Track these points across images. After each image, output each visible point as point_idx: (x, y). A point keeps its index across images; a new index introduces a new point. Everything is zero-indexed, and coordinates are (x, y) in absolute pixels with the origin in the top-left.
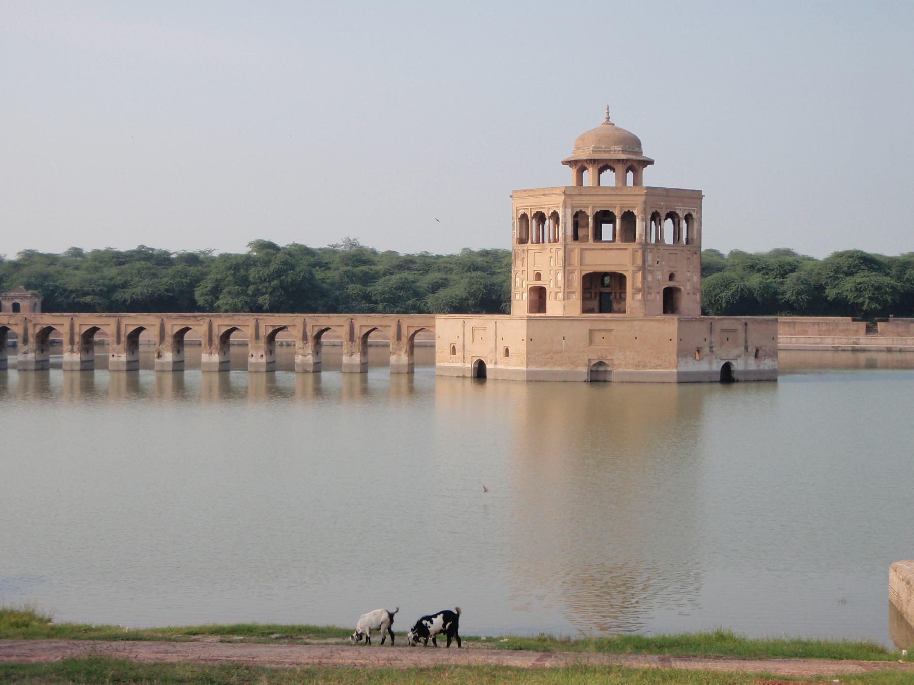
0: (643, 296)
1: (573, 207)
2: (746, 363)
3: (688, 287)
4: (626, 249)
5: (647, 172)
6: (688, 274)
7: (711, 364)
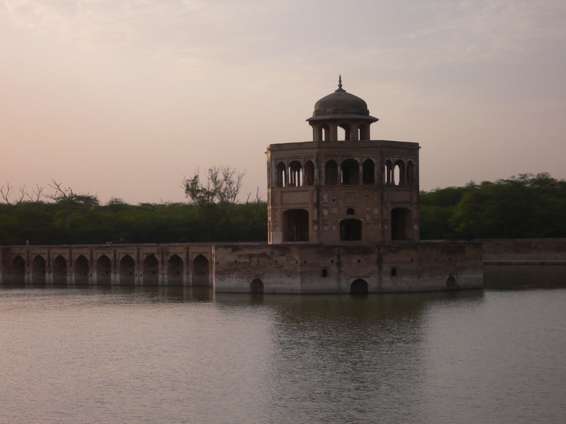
0: (318, 227)
1: (276, 160)
2: (380, 280)
3: (368, 218)
4: (307, 191)
5: (373, 126)
6: (368, 208)
7: (339, 280)
